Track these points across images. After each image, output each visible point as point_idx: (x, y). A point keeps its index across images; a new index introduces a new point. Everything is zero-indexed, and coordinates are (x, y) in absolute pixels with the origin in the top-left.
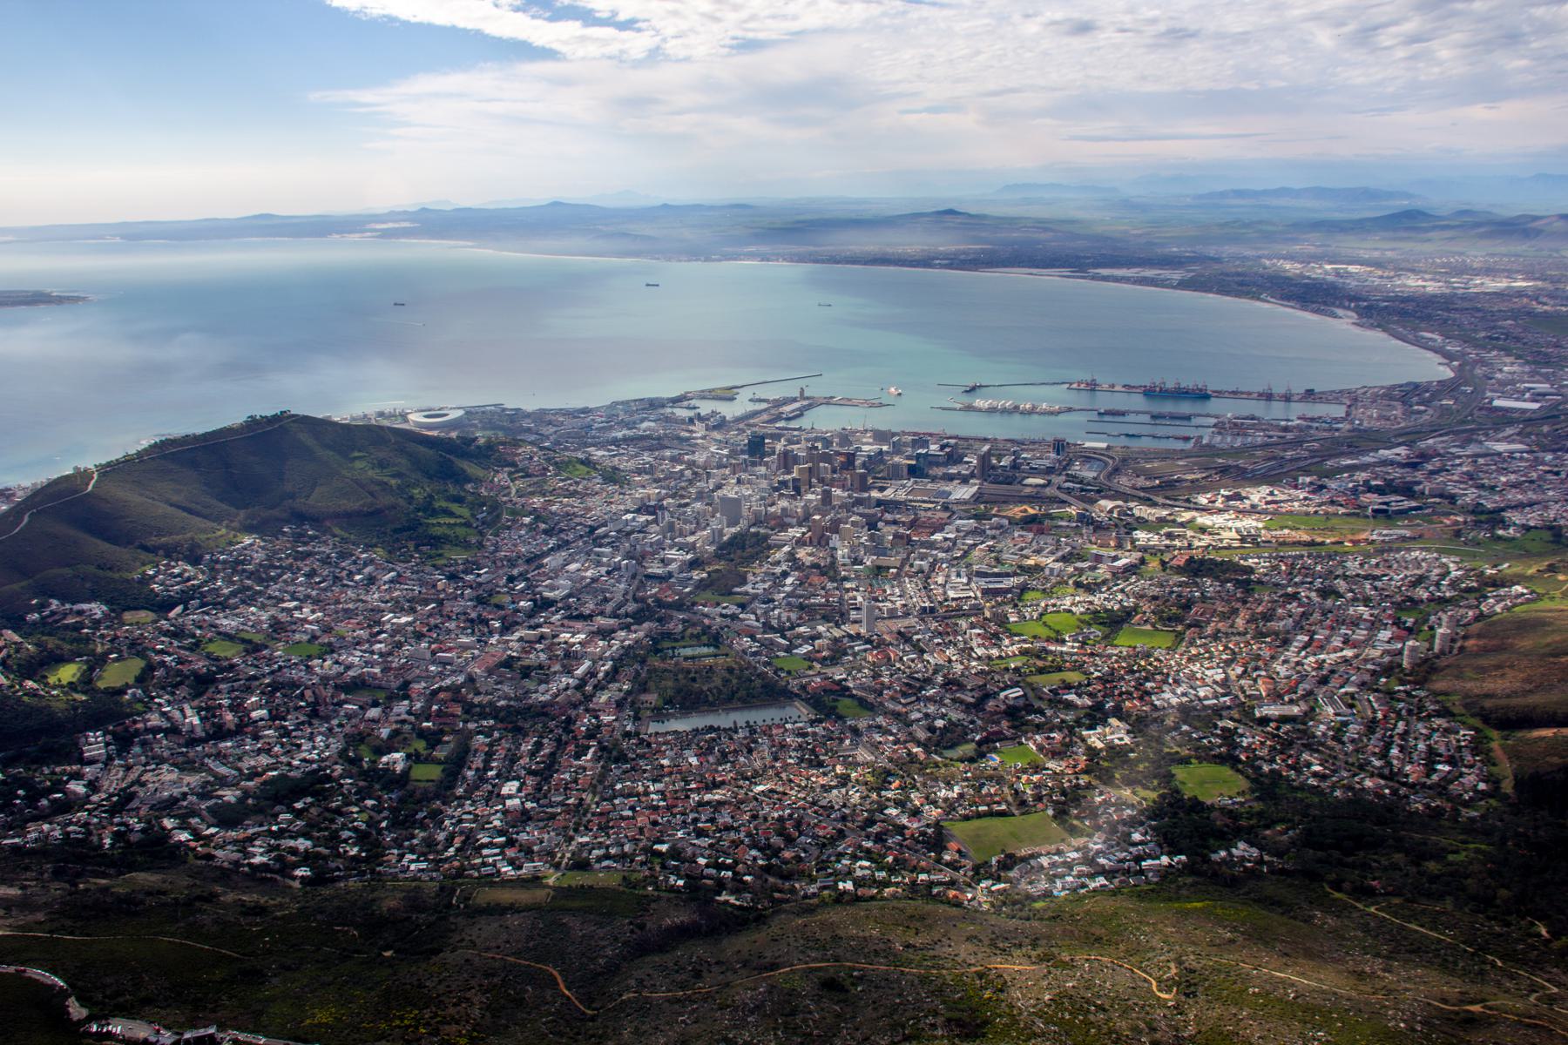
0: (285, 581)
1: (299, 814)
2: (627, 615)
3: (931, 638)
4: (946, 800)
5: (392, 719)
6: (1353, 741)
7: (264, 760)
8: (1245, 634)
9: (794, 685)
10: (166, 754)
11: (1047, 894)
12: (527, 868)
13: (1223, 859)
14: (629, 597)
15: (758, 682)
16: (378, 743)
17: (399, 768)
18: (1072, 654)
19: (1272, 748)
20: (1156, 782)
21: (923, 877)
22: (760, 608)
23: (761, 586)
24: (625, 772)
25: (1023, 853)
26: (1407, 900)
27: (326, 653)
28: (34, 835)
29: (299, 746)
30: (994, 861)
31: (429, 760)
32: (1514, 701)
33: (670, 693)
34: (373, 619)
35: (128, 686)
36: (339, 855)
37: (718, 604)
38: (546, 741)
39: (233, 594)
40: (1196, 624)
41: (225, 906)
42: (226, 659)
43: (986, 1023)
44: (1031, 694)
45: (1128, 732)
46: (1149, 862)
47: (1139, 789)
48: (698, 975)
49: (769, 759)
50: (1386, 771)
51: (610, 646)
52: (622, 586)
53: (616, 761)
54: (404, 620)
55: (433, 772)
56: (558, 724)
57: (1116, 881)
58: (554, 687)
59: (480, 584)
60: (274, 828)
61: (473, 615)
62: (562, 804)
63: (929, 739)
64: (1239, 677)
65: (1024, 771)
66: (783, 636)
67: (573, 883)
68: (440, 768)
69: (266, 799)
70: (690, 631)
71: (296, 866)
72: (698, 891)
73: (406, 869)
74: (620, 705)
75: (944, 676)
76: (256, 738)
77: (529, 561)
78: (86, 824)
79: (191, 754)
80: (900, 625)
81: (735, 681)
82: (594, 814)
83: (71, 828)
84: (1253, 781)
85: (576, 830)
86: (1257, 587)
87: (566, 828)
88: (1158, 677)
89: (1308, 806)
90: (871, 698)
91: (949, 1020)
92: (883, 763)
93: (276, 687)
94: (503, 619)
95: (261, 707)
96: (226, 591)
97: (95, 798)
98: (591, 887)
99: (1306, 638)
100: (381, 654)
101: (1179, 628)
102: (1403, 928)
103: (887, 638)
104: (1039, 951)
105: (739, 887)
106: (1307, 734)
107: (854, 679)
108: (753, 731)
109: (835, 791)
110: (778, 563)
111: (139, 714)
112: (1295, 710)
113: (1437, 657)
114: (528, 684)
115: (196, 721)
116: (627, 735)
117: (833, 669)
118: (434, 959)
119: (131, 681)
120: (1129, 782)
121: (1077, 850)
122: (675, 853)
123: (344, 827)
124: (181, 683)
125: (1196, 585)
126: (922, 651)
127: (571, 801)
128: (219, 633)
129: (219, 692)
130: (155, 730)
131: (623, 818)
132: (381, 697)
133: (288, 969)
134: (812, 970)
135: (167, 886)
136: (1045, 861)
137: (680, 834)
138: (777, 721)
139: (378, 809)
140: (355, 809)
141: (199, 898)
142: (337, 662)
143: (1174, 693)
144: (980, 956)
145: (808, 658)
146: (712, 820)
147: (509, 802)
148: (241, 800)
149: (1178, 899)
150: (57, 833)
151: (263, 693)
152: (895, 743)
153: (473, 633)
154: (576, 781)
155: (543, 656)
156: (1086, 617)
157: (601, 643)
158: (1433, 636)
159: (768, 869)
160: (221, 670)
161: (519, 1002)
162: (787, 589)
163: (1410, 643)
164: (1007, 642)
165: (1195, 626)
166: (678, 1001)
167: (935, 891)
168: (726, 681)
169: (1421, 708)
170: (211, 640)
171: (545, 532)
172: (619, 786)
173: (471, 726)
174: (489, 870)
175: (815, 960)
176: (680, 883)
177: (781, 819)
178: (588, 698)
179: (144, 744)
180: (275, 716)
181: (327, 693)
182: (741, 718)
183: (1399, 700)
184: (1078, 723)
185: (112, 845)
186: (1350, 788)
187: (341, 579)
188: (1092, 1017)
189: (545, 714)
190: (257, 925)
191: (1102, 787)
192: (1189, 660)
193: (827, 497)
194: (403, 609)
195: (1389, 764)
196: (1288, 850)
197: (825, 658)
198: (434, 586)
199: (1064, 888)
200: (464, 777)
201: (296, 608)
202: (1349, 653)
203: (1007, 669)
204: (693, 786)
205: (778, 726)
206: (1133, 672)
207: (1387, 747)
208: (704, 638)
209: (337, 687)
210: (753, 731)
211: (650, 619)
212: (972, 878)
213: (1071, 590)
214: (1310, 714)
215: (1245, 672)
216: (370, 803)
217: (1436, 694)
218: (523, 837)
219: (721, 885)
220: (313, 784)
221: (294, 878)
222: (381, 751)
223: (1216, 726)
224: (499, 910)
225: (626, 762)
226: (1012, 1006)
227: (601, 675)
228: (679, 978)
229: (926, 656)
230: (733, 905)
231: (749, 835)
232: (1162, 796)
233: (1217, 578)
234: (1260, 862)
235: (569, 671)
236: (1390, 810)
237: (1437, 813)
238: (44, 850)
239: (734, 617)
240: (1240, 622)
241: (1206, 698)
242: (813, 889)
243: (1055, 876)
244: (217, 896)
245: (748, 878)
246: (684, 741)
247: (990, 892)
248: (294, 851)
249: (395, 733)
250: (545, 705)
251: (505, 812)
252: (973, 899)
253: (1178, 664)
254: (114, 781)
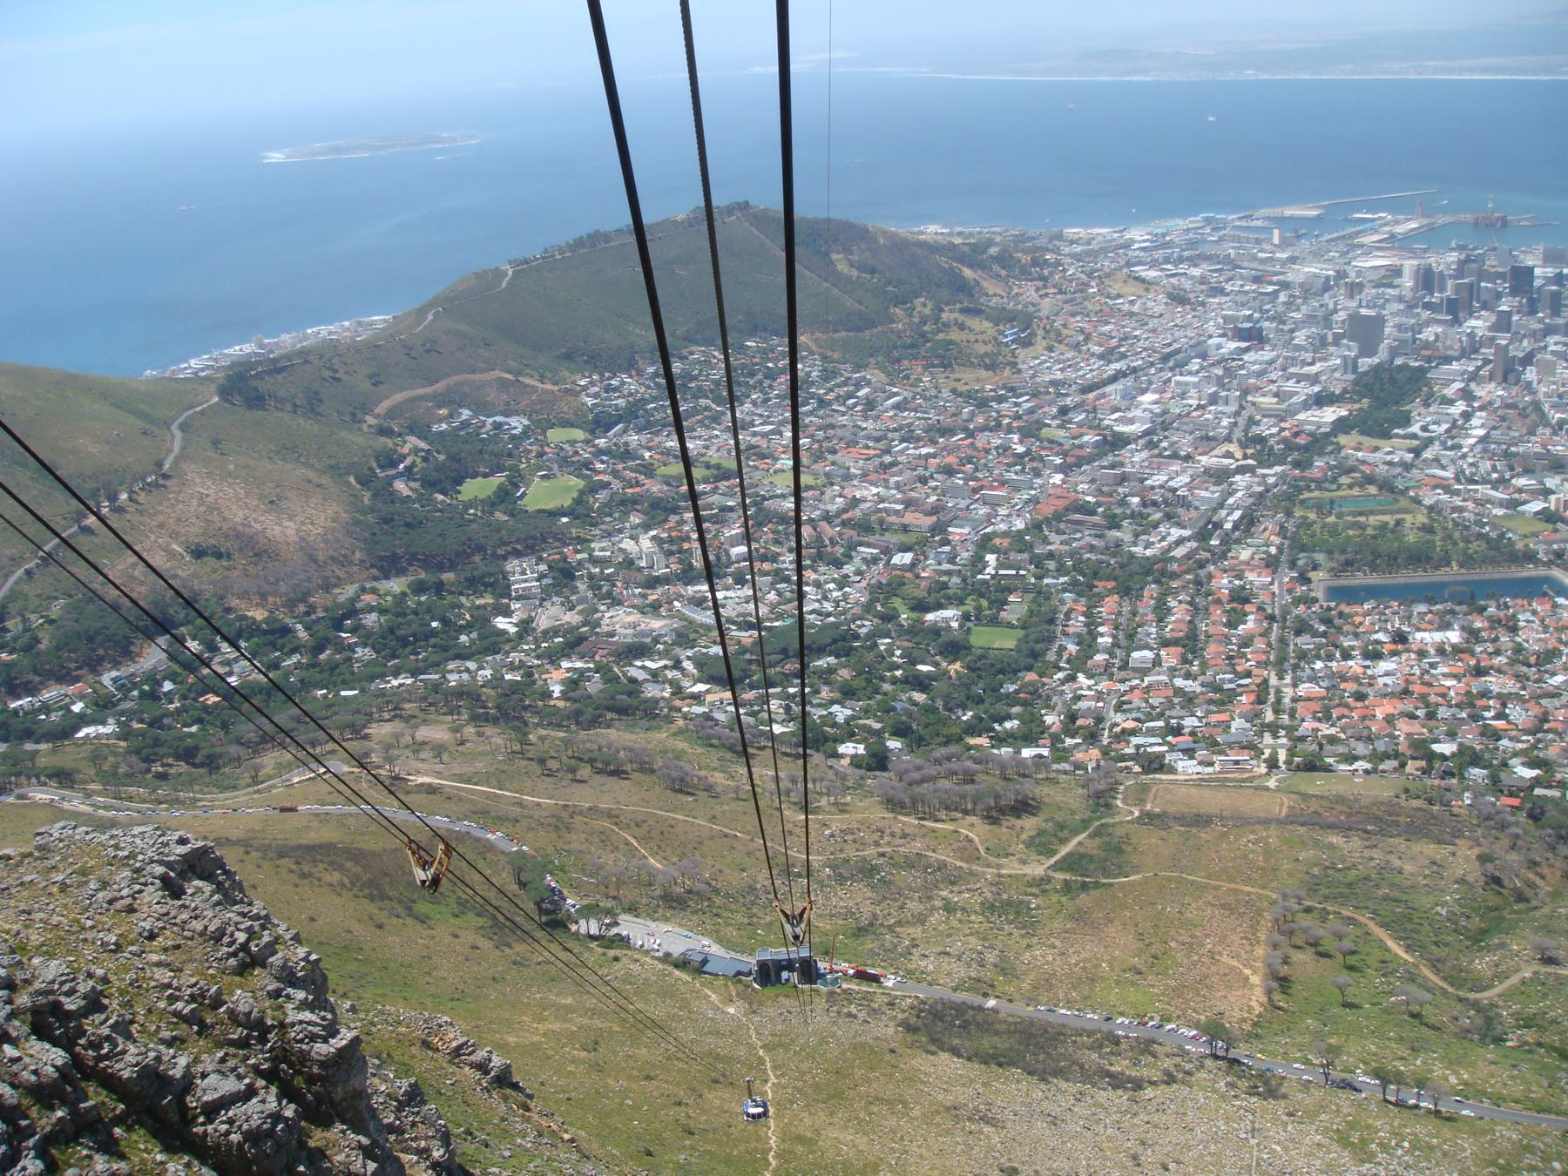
31: (994, 621)
37: (1376, 449)
68: (1021, 633)
77: (1085, 390)
110: (1451, 402)
162: (1481, 432)
171: (1101, 357)
187: (830, 403)
193: (1503, 323)
201: (772, 432)
209: (844, 524)
220: (835, 641)
227: (1228, 526)
238: (467, 694)
248: (830, 720)
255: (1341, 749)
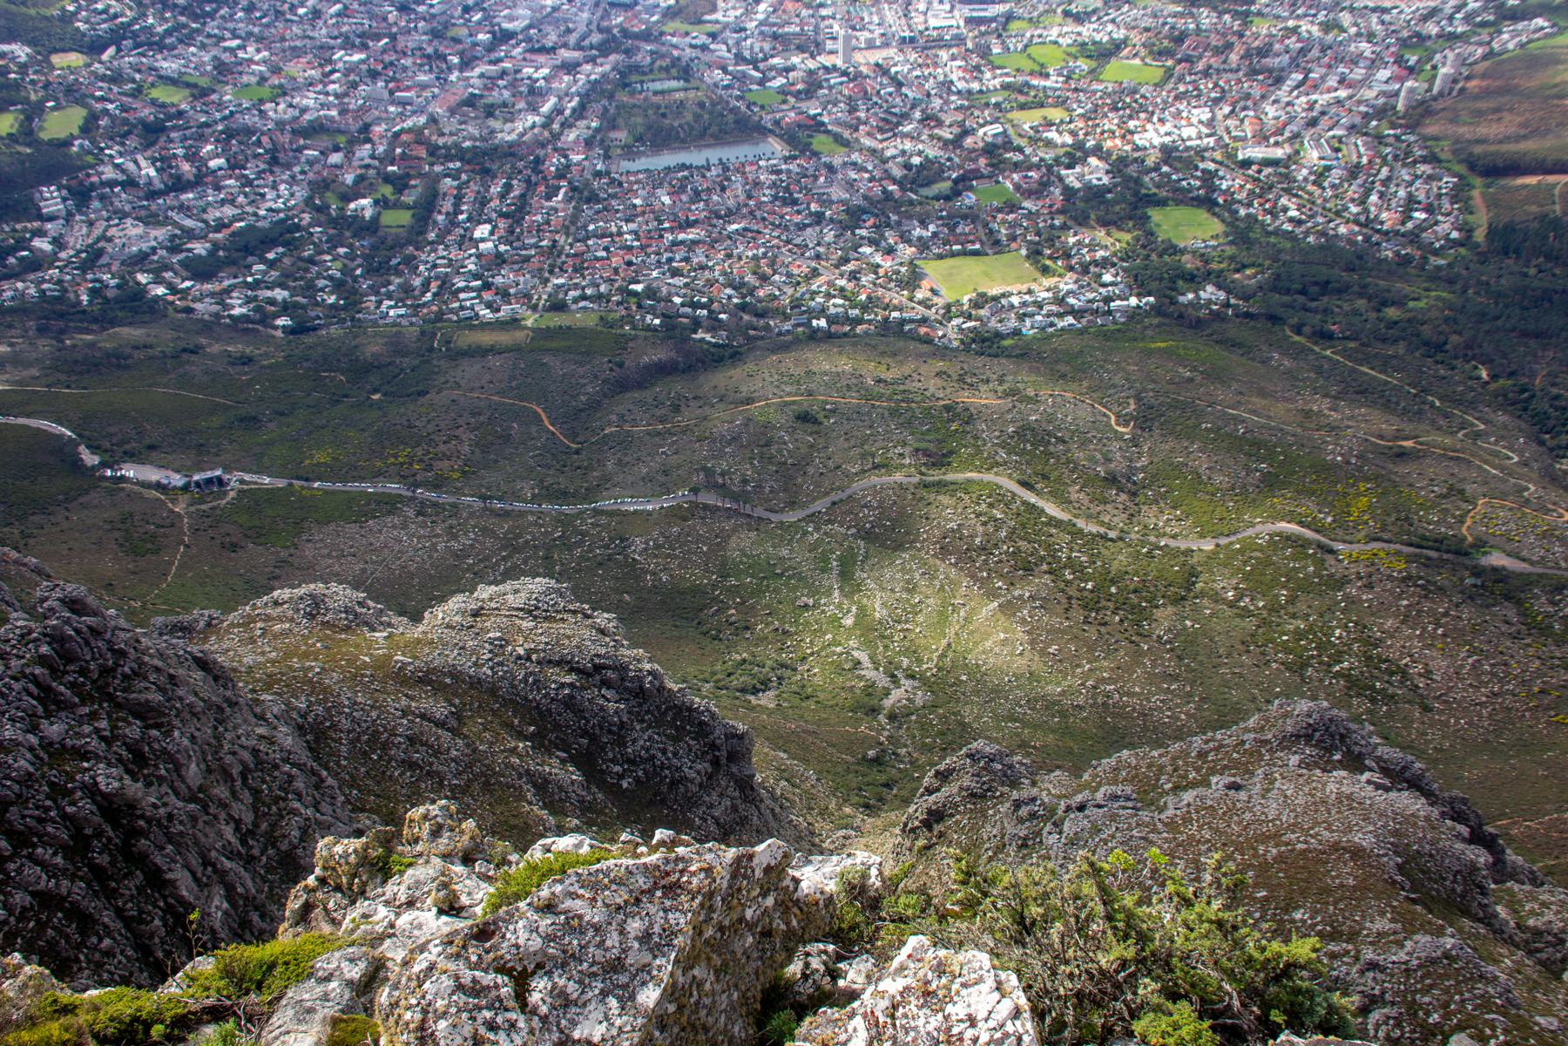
0: (223, 17)
1: (272, 264)
2: (592, 47)
3: (910, 71)
4: (920, 238)
5: (355, 164)
6: (1333, 186)
7: (229, 211)
8: (1237, 71)
9: (767, 120)
10: (127, 208)
11: (1017, 332)
12: (505, 311)
13: (1190, 303)
14: (593, 27)
15: (731, 118)
16: (342, 189)
17: (368, 214)
18: (1056, 90)
19: (1251, 193)
20: (1131, 224)
21: (895, 314)
22: (732, 37)
23: (732, 13)
24: (597, 212)
25: (994, 291)
26: (1363, 345)
27: (278, 96)
28: (9, 294)
29: (263, 195)
30: (965, 300)
31: (397, 205)
32: (1505, 148)
33: (640, 129)
34: (323, 54)
35: (73, 137)
36: (317, 304)
37: (687, 34)
38: (515, 182)
39: (168, 33)
40: (1187, 59)
41: (213, 357)
42: (173, 105)
43: (951, 453)
44: (1011, 132)
45: (1107, 172)
46: (1118, 303)
47: (1113, 230)
48: (676, 409)
49: (742, 197)
50: (1362, 218)
51: (576, 81)
52: (585, 15)
53: (588, 201)
54: (357, 57)
55: (405, 217)
56: (526, 163)
57: (1084, 321)
58: (519, 126)
59: (434, 16)
60: (250, 279)
61: (430, 50)
62: (536, 246)
63: (905, 176)
64: (1226, 117)
65: (999, 210)
66: (756, 69)
67: (552, 325)
68: (410, 213)
69: (237, 250)
70: (658, 63)
71: (276, 316)
72: (674, 329)
73: (385, 316)
74: (589, 143)
75: (923, 111)
76: (218, 188)
78: (60, 282)
79: (154, 208)
80: (877, 56)
81: (706, 117)
82: (568, 256)
83: (45, 286)
84: (1228, 224)
85: (551, 272)
86: (1257, 20)
87: (541, 270)
88: (1143, 116)
89: (1280, 251)
90: (846, 134)
91: (917, 450)
92: (857, 201)
93: (230, 134)
94: (461, 54)
95: (218, 156)
96: (160, 30)
97: (63, 255)
98: (569, 328)
99: (1301, 77)
100: (337, 96)
101: (1170, 63)
102: (1354, 371)
103: (864, 70)
104: (1006, 386)
105: (714, 325)
106: (1287, 178)
107: (829, 114)
108: (726, 169)
109: (809, 230)
111: (92, 167)
112: (1279, 153)
113: (1435, 99)
114: (492, 123)
115: (153, 173)
116: (598, 174)
117: (808, 104)
118: (422, 400)
119: (76, 132)
120: (1105, 223)
121: (1048, 290)
122: (651, 293)
123: (319, 276)
124: (130, 133)
125: (1192, 15)
126: (900, 85)
127: (544, 243)
128: (161, 77)
129: (171, 141)
130: (112, 184)
131: (597, 259)
132: (341, 140)
133: (282, 414)
134: (786, 404)
135: (151, 340)
136: (1015, 300)
137: (655, 274)
138: (750, 158)
139: (351, 257)
140: (328, 258)
141: (184, 350)
142: (291, 106)
143: (1156, 131)
144: (948, 391)
145: (782, 91)
146: (687, 260)
147: (482, 246)
148: (212, 253)
149: (1143, 339)
150: (32, 291)
151: (217, 141)
152: (871, 180)
153: (431, 71)
154: (548, 223)
155: (506, 94)
156: (1073, 50)
157: (566, 78)
158: (1434, 77)
159: (743, 307)
160: (170, 118)
161: (507, 438)
162: (760, 17)
163: (1409, 84)
164: (988, 75)
165: (1186, 61)
166: (659, 434)
167: (907, 328)
168: (697, 117)
169: (1408, 154)
170: (153, 85)
172: (591, 227)
173: (438, 169)
174: (467, 313)
175: (789, 394)
176: (657, 321)
177: (755, 258)
178: (556, 137)
179: (102, 198)
180: (234, 165)
181: (286, 139)
182: (713, 155)
183: (1386, 145)
184: (1057, 160)
185: (90, 302)
186: (1323, 234)
187: (283, 14)
188: (1051, 448)
189: (513, 155)
190: (246, 374)
191: (1077, 228)
192: (1177, 98)
194: (353, 46)
195: (1366, 211)
196: (1254, 295)
197: (799, 92)
198: (385, 19)
199: (1032, 327)
200: (435, 222)
201: (239, 48)
202: (1343, 93)
203: (987, 105)
204: (666, 225)
205: (752, 164)
206: (1116, 109)
207: (1367, 194)
208: (674, 72)
209: (293, 131)
210: (726, 169)
211: (617, 51)
212: (944, 316)
213: (1059, 18)
214: (1294, 157)
215: (1232, 112)
216: (342, 251)
217: (1425, 138)
218: (499, 280)
219: (696, 324)
221: (276, 328)
222: (347, 198)
223: (1196, 168)
224: (482, 352)
225: (598, 202)
226: (976, 438)
227: (568, 112)
228: (658, 412)
229: (904, 90)
230: (709, 343)
231: (724, 273)
232: (1137, 239)
233: (1215, 9)
234: (1227, 305)
235: (534, 109)
236: (1360, 258)
237: (1405, 261)
238: (22, 309)
239: (704, 48)
240: (1234, 57)
241: (1190, 139)
242: (787, 326)
243: (1025, 315)
244: (202, 347)
245: (722, 316)
246: (656, 180)
247: (961, 329)
248: (272, 302)
249: (361, 179)
250: (511, 145)
251: (479, 256)
252: (944, 336)
253: (1165, 102)
254: (79, 237)
255: (577, 293)
